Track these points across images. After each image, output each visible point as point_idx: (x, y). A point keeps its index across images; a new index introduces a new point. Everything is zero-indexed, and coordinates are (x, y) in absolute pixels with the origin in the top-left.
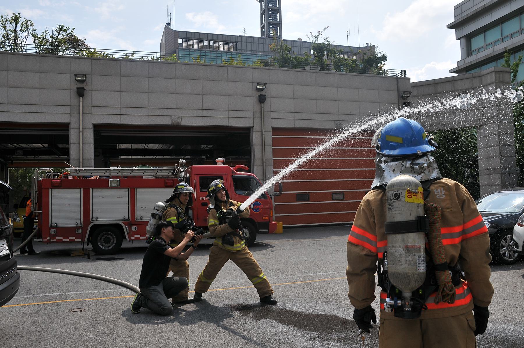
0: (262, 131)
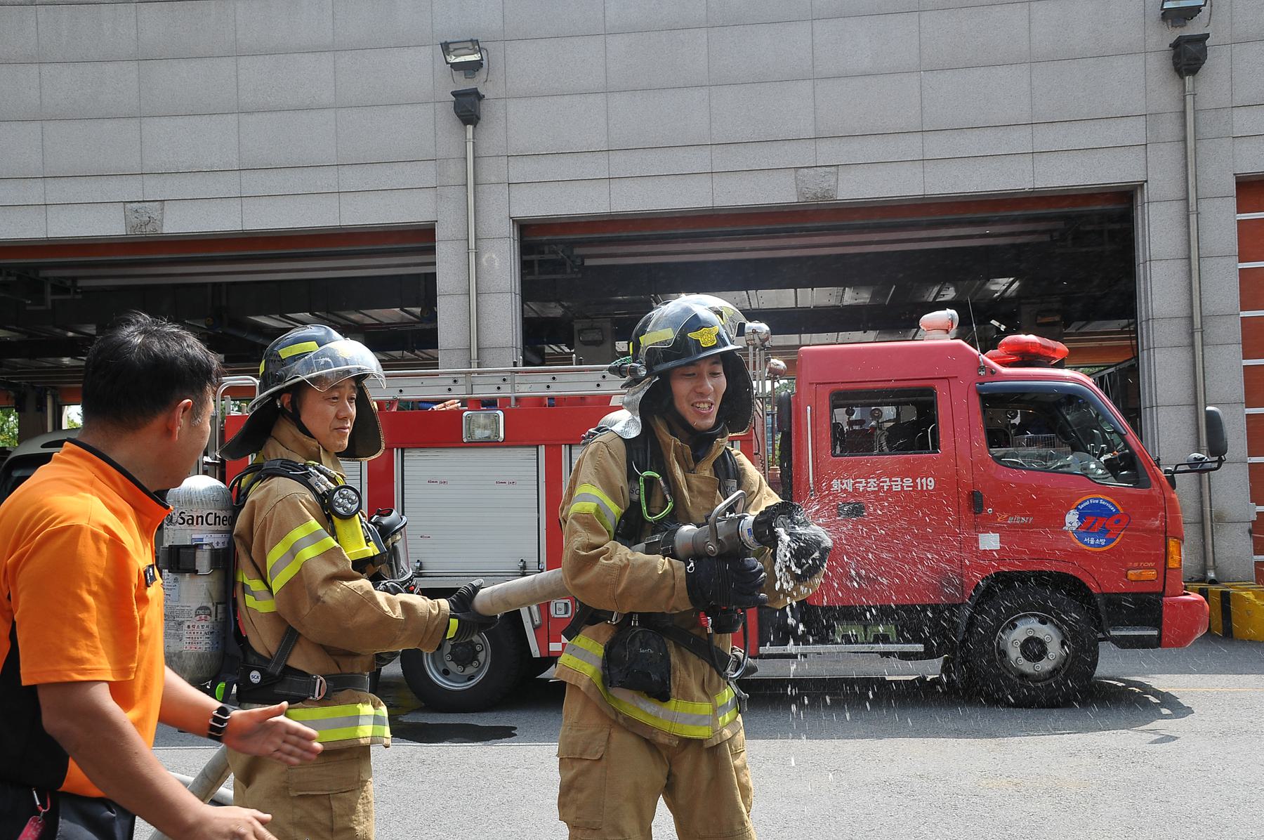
0: (1187, 199)
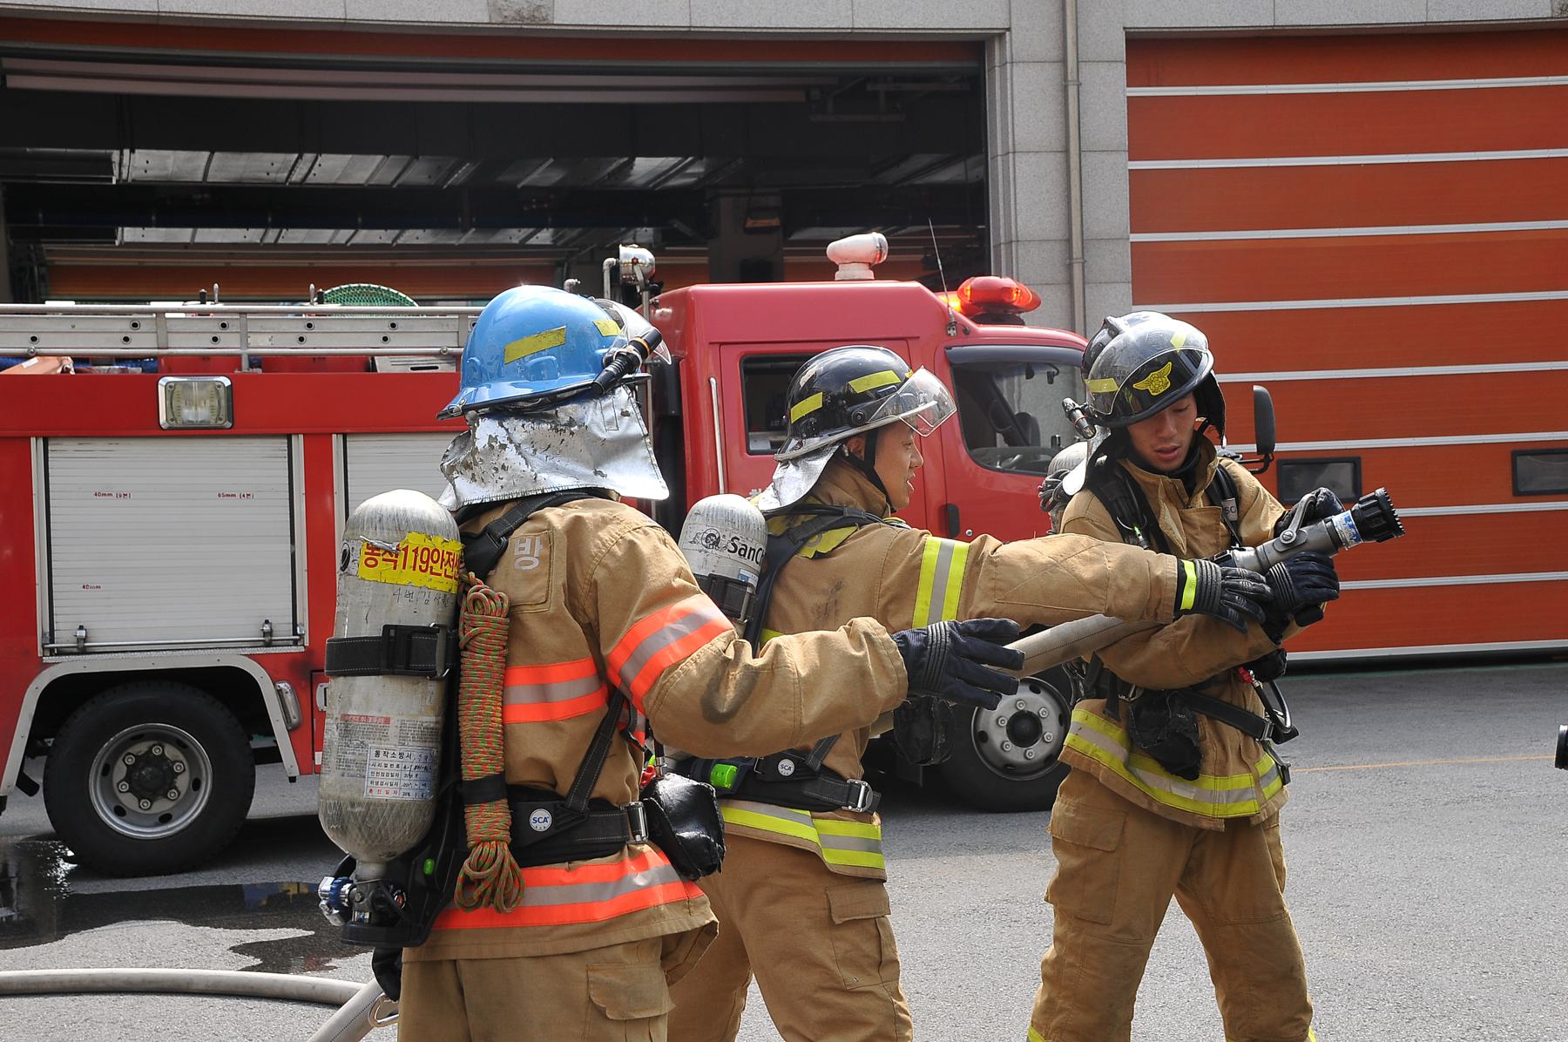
0: (1064, 61)
